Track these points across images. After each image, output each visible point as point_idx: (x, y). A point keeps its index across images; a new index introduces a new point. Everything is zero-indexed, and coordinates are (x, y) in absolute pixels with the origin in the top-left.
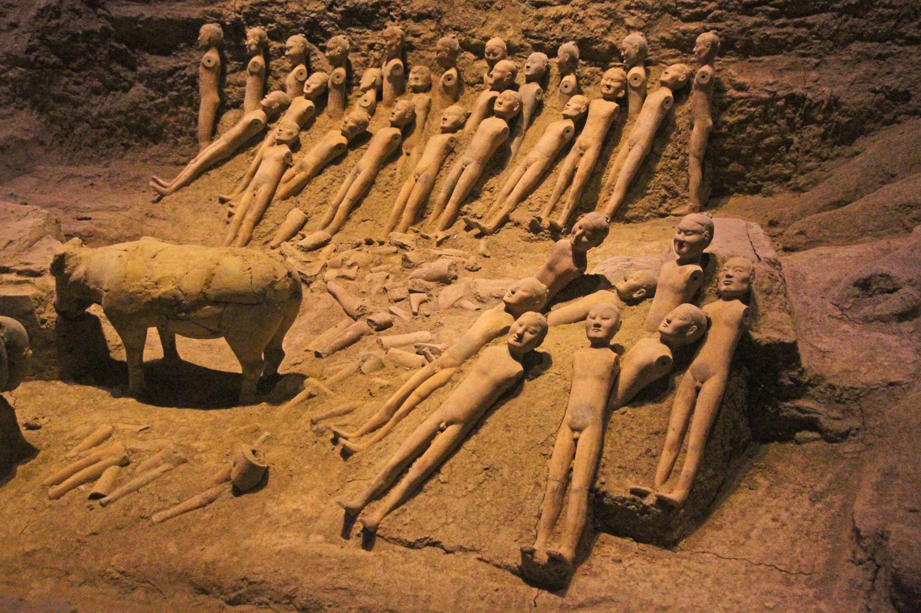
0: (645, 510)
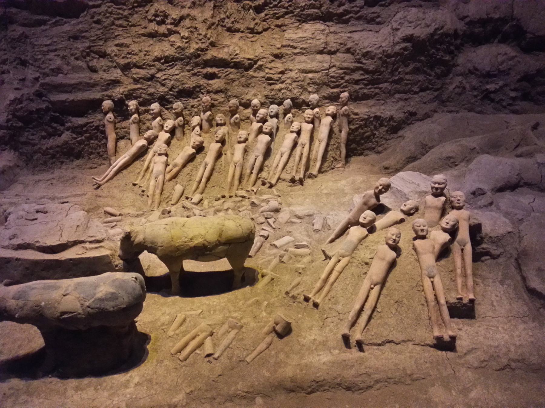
0: (465, 305)
